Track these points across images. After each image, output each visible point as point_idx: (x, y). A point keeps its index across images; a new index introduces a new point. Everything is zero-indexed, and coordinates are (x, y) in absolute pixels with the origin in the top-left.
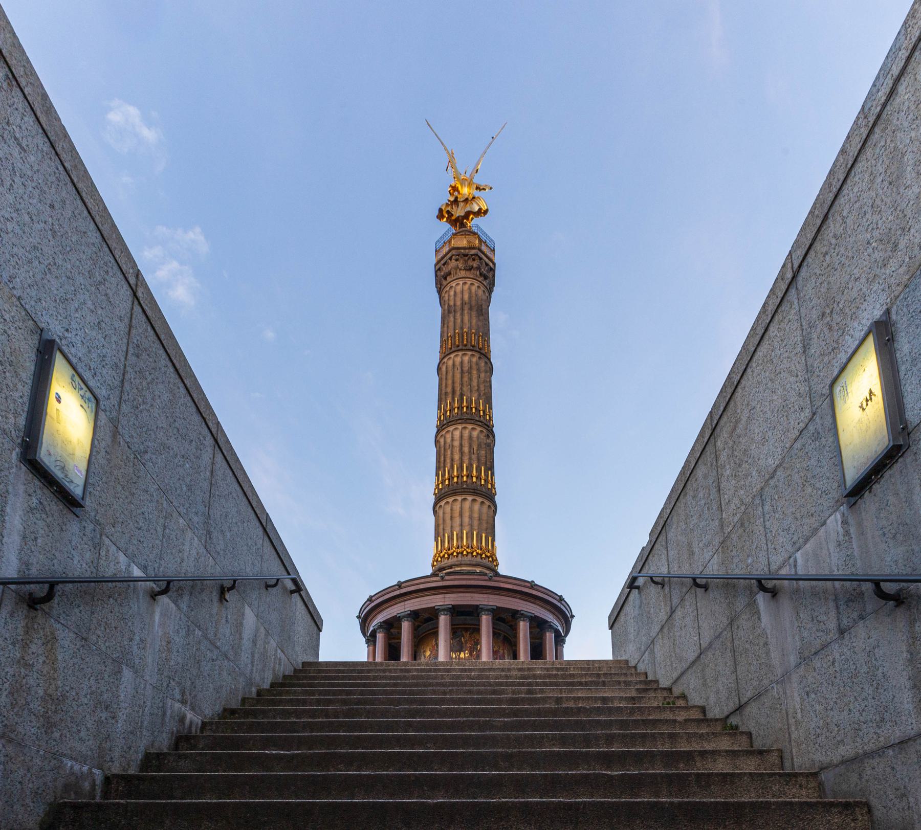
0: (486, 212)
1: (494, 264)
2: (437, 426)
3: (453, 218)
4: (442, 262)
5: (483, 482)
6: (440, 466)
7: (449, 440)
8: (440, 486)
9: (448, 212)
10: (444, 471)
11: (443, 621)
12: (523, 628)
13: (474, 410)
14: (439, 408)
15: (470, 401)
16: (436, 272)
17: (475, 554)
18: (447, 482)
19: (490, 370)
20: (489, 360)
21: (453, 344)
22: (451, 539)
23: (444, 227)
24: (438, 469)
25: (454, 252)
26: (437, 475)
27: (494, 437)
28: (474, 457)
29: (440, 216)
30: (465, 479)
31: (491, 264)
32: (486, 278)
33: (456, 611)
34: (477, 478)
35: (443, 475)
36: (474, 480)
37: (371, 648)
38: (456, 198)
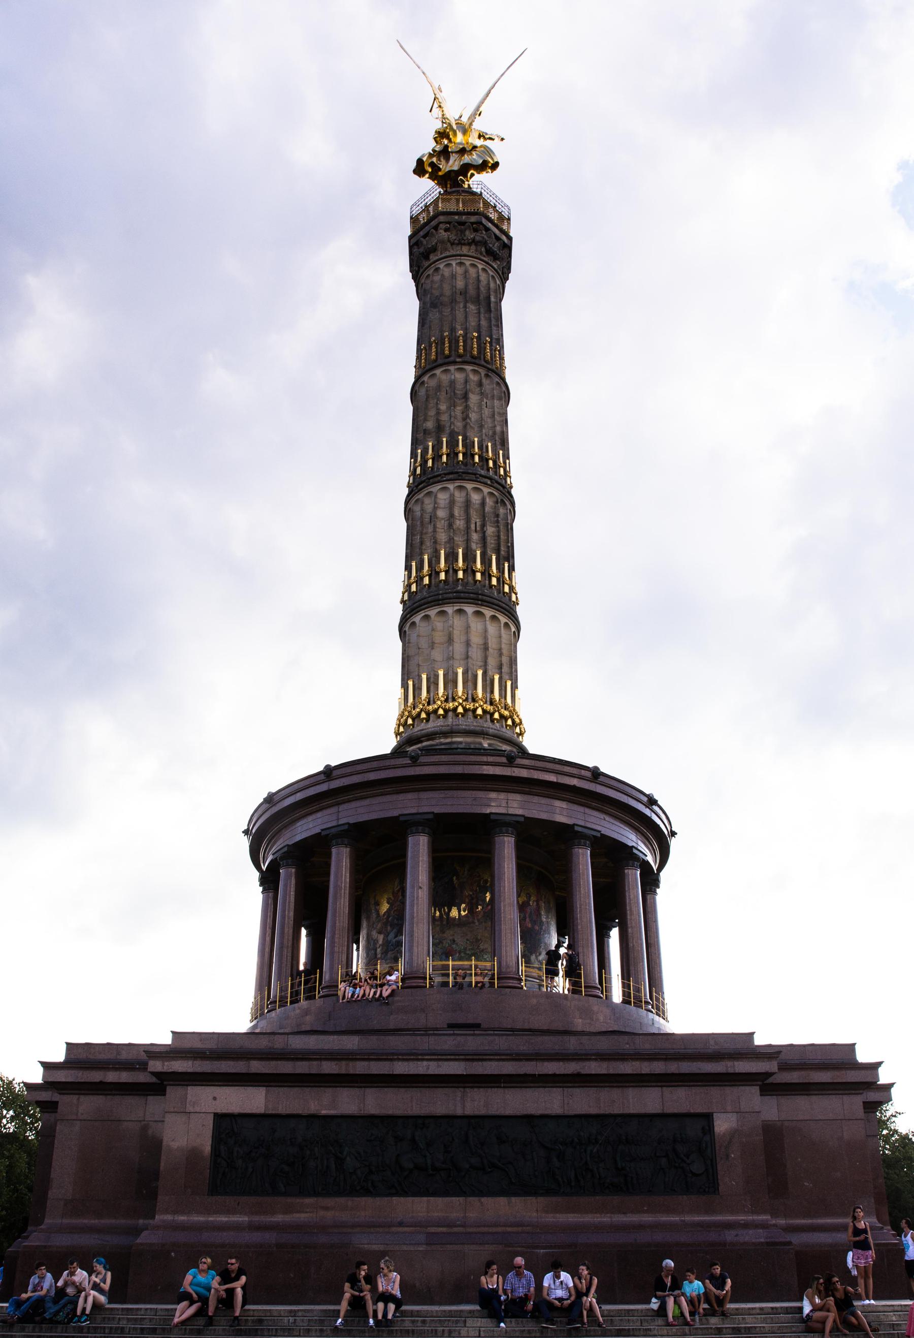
0: (495, 166)
1: (510, 239)
2: (408, 486)
3: (440, 173)
4: (422, 233)
5: (494, 581)
6: (413, 552)
7: (429, 507)
8: (414, 588)
9: (432, 165)
10: (422, 561)
11: (419, 848)
12: (584, 859)
13: (477, 459)
14: (413, 455)
15: (468, 445)
16: (411, 248)
17: (479, 711)
18: (426, 581)
19: (506, 396)
20: (503, 380)
21: (440, 352)
22: (433, 683)
23: (427, 188)
24: (409, 558)
25: (442, 218)
26: (408, 568)
27: (513, 504)
28: (475, 537)
29: (420, 170)
30: (460, 575)
31: (504, 238)
32: (495, 257)
33: (442, 827)
34: (483, 574)
35: (420, 568)
36: (478, 576)
37: (271, 895)
38: (446, 147)
